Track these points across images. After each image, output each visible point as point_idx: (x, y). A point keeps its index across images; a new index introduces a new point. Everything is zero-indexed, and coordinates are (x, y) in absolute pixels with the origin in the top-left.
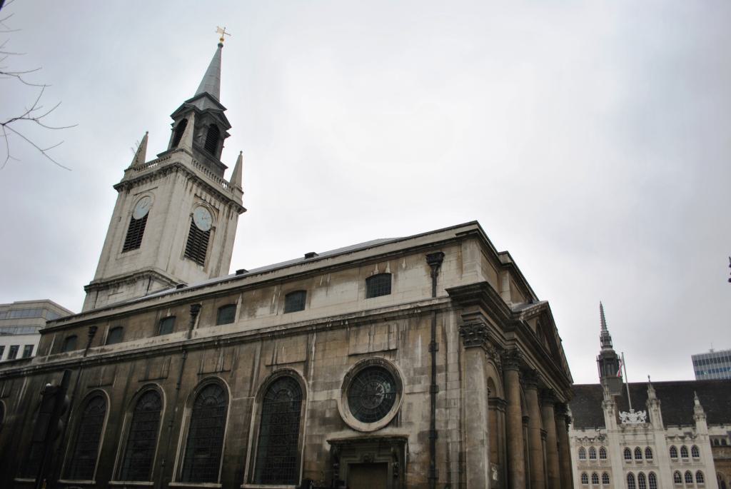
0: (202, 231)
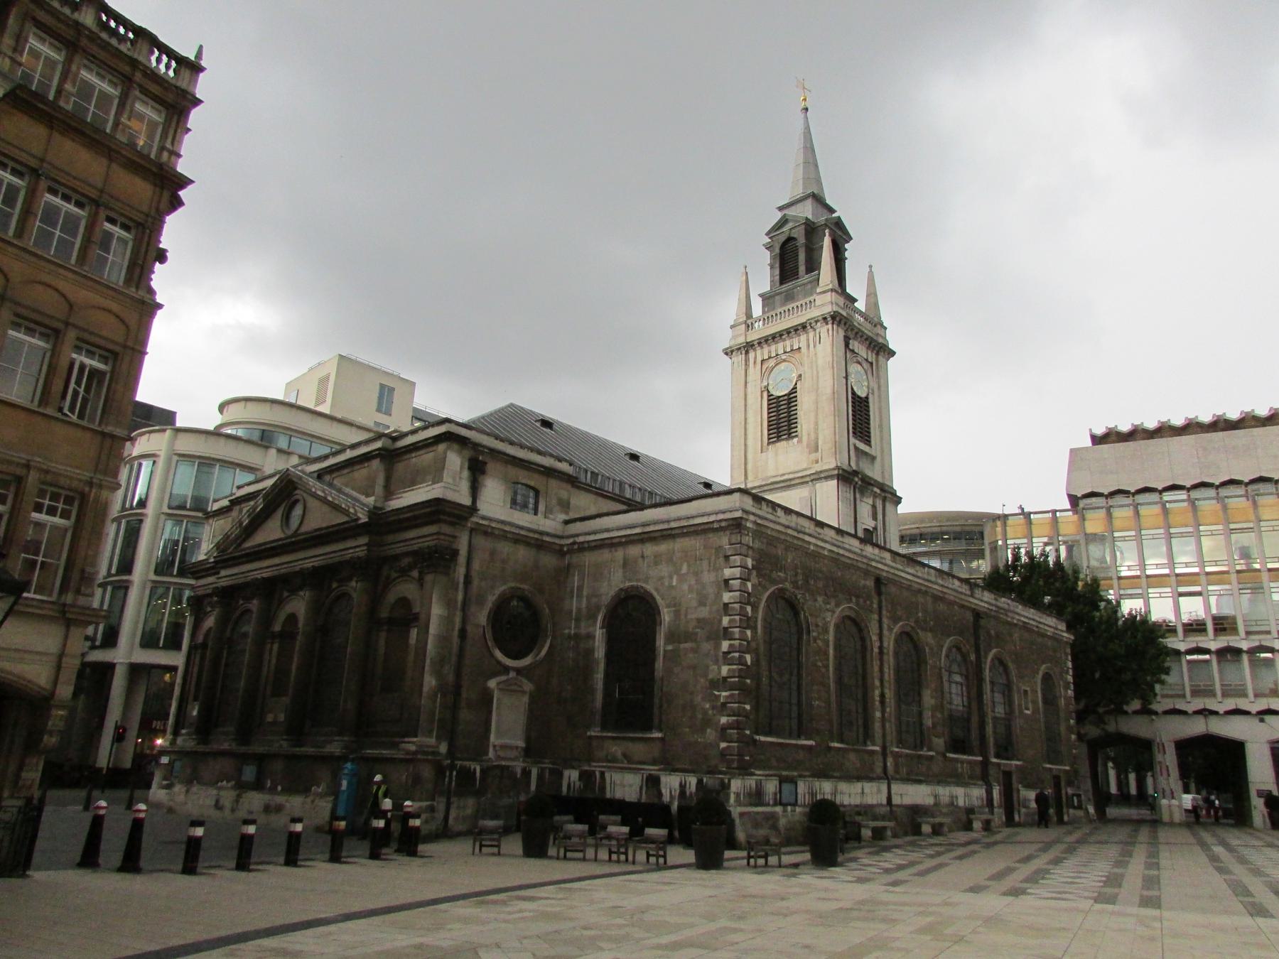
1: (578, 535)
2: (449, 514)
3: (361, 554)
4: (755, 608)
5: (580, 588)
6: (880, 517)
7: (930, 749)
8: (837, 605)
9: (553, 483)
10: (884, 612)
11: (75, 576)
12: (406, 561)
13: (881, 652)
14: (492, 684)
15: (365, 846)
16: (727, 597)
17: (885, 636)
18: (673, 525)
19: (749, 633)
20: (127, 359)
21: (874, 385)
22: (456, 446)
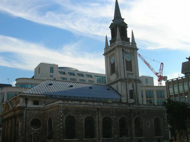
6: (135, 86)
10: (100, 114)
14: (32, 133)
17: (99, 119)
19: (61, 123)
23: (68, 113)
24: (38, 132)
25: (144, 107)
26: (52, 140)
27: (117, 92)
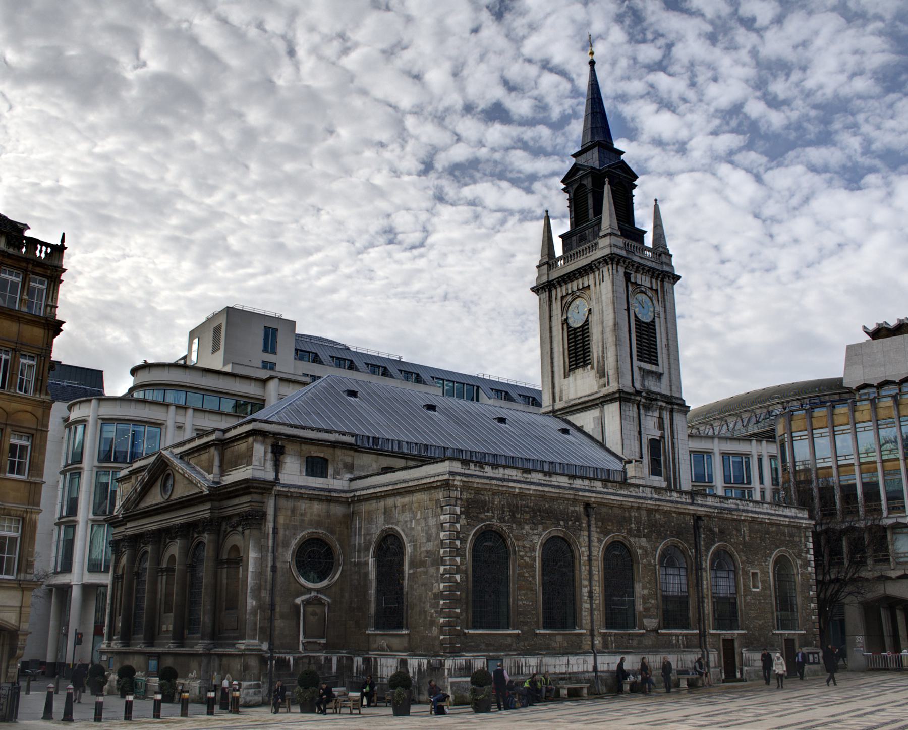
0: (646, 323)
1: (356, 490)
2: (257, 488)
3: (207, 515)
4: (463, 541)
5: (360, 528)
7: (640, 629)
8: (544, 530)
9: (339, 452)
10: (593, 529)
11: (24, 563)
12: (235, 520)
13: (590, 560)
14: (298, 601)
15: (205, 708)
16: (442, 534)
17: (591, 549)
18: (411, 484)
19: (458, 560)
20: (39, 436)
21: (659, 308)
22: (260, 438)
23: (482, 516)
24: (323, 597)
25: (743, 511)
26: (405, 632)
27: (602, 445)
